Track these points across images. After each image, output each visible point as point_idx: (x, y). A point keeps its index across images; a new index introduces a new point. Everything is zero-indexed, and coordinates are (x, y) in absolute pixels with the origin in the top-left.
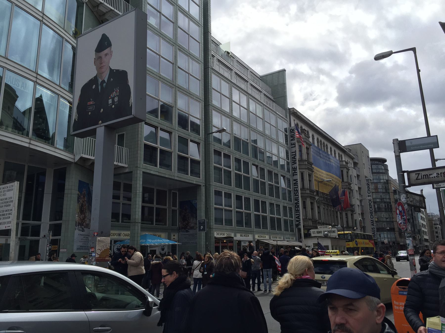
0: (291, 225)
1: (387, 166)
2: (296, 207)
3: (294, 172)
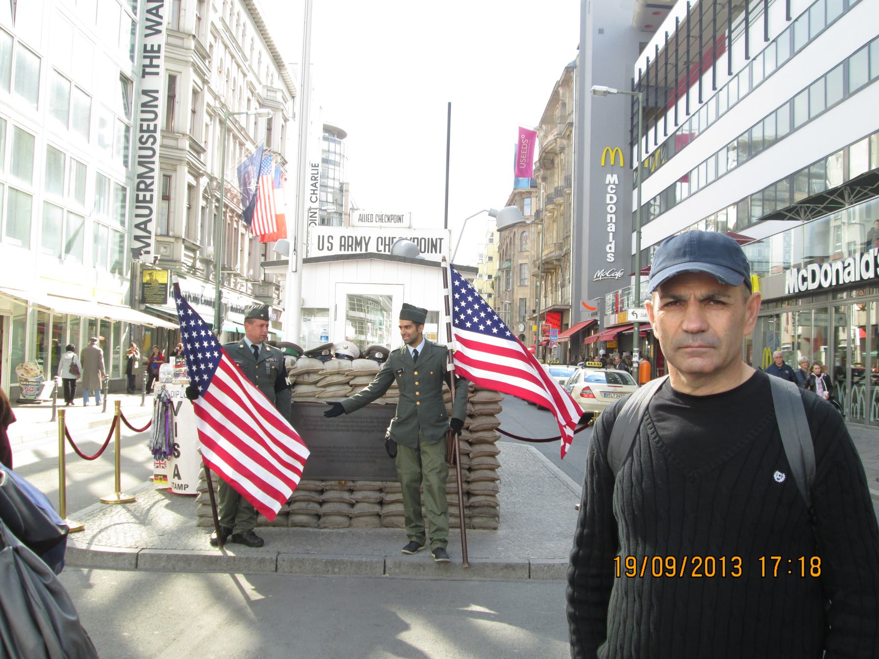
2: (139, 189)
3: (147, 62)
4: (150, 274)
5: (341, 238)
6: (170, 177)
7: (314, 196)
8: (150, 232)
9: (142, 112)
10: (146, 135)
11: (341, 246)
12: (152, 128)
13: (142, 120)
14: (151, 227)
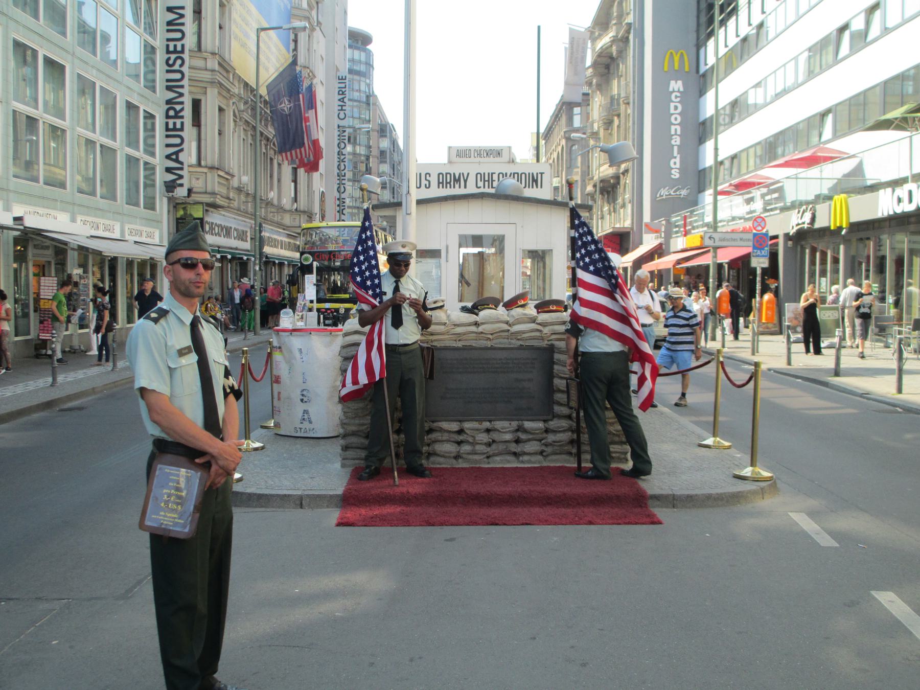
0: (150, 184)
1: (369, 54)
2: (168, 117)
4: (184, 209)
5: (439, 175)
6: (199, 101)
7: (342, 112)
8: (182, 163)
9: (168, 31)
10: (173, 56)
11: (439, 183)
12: (179, 49)
13: (168, 40)
14: (182, 157)
